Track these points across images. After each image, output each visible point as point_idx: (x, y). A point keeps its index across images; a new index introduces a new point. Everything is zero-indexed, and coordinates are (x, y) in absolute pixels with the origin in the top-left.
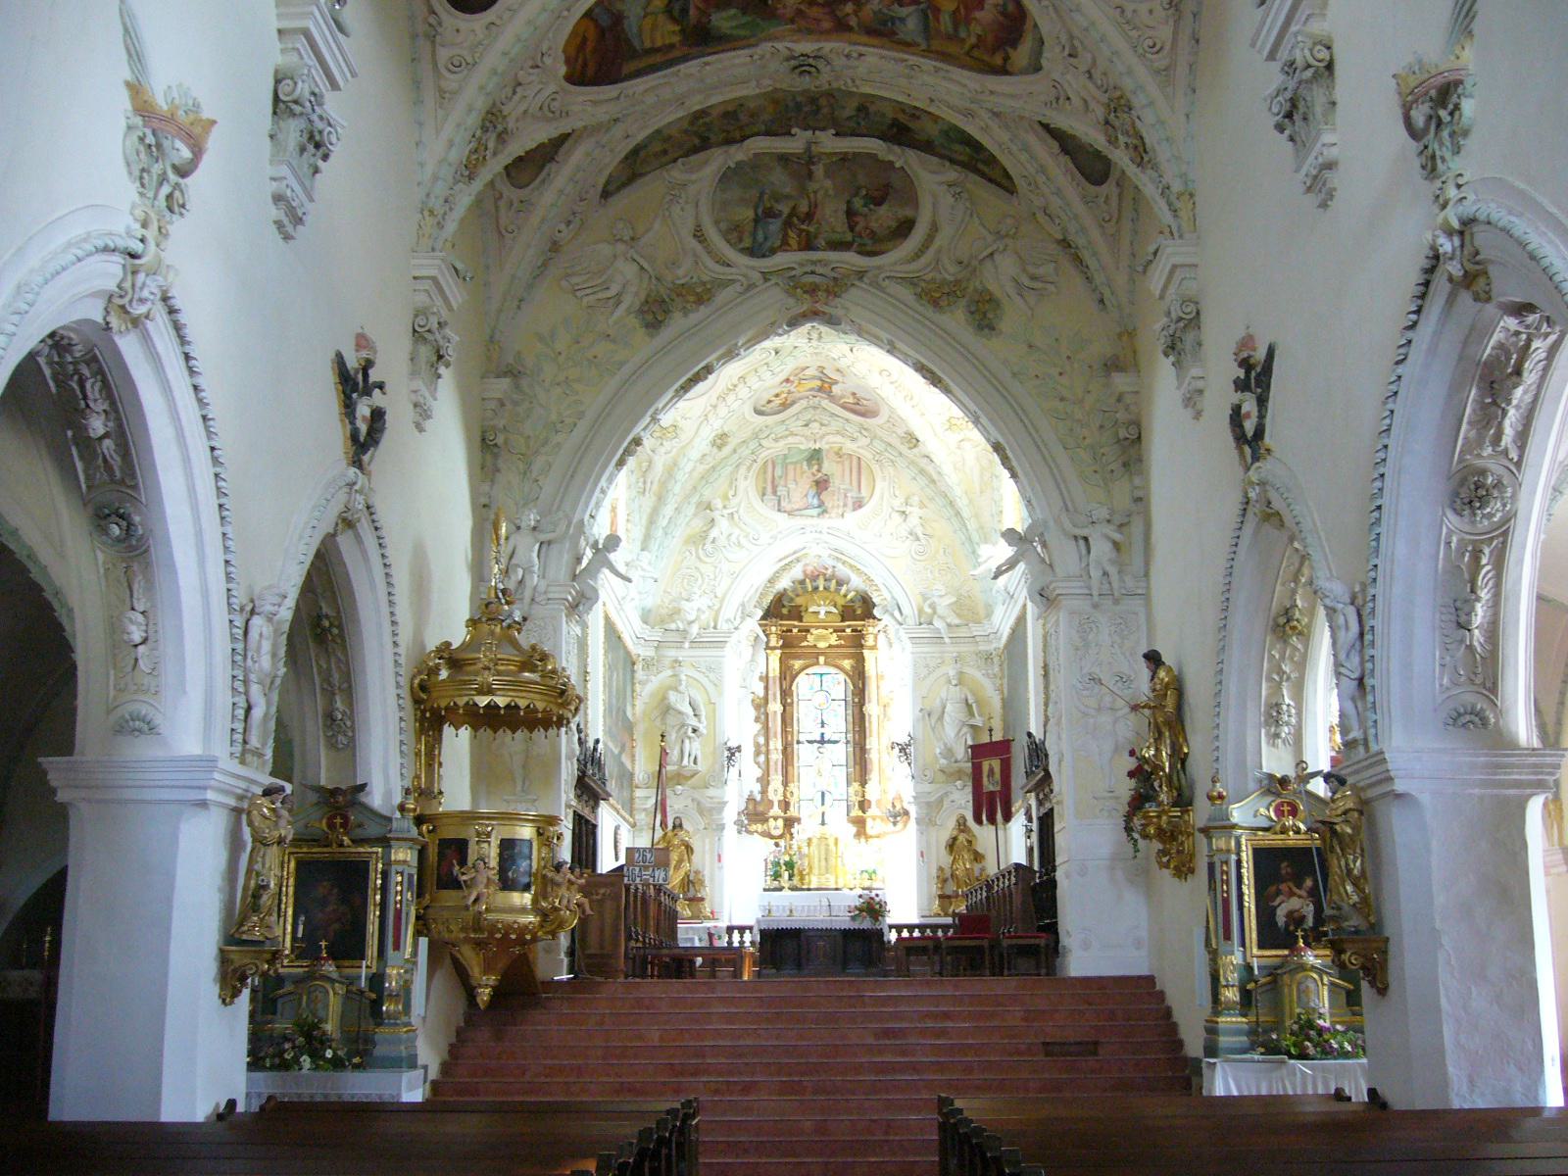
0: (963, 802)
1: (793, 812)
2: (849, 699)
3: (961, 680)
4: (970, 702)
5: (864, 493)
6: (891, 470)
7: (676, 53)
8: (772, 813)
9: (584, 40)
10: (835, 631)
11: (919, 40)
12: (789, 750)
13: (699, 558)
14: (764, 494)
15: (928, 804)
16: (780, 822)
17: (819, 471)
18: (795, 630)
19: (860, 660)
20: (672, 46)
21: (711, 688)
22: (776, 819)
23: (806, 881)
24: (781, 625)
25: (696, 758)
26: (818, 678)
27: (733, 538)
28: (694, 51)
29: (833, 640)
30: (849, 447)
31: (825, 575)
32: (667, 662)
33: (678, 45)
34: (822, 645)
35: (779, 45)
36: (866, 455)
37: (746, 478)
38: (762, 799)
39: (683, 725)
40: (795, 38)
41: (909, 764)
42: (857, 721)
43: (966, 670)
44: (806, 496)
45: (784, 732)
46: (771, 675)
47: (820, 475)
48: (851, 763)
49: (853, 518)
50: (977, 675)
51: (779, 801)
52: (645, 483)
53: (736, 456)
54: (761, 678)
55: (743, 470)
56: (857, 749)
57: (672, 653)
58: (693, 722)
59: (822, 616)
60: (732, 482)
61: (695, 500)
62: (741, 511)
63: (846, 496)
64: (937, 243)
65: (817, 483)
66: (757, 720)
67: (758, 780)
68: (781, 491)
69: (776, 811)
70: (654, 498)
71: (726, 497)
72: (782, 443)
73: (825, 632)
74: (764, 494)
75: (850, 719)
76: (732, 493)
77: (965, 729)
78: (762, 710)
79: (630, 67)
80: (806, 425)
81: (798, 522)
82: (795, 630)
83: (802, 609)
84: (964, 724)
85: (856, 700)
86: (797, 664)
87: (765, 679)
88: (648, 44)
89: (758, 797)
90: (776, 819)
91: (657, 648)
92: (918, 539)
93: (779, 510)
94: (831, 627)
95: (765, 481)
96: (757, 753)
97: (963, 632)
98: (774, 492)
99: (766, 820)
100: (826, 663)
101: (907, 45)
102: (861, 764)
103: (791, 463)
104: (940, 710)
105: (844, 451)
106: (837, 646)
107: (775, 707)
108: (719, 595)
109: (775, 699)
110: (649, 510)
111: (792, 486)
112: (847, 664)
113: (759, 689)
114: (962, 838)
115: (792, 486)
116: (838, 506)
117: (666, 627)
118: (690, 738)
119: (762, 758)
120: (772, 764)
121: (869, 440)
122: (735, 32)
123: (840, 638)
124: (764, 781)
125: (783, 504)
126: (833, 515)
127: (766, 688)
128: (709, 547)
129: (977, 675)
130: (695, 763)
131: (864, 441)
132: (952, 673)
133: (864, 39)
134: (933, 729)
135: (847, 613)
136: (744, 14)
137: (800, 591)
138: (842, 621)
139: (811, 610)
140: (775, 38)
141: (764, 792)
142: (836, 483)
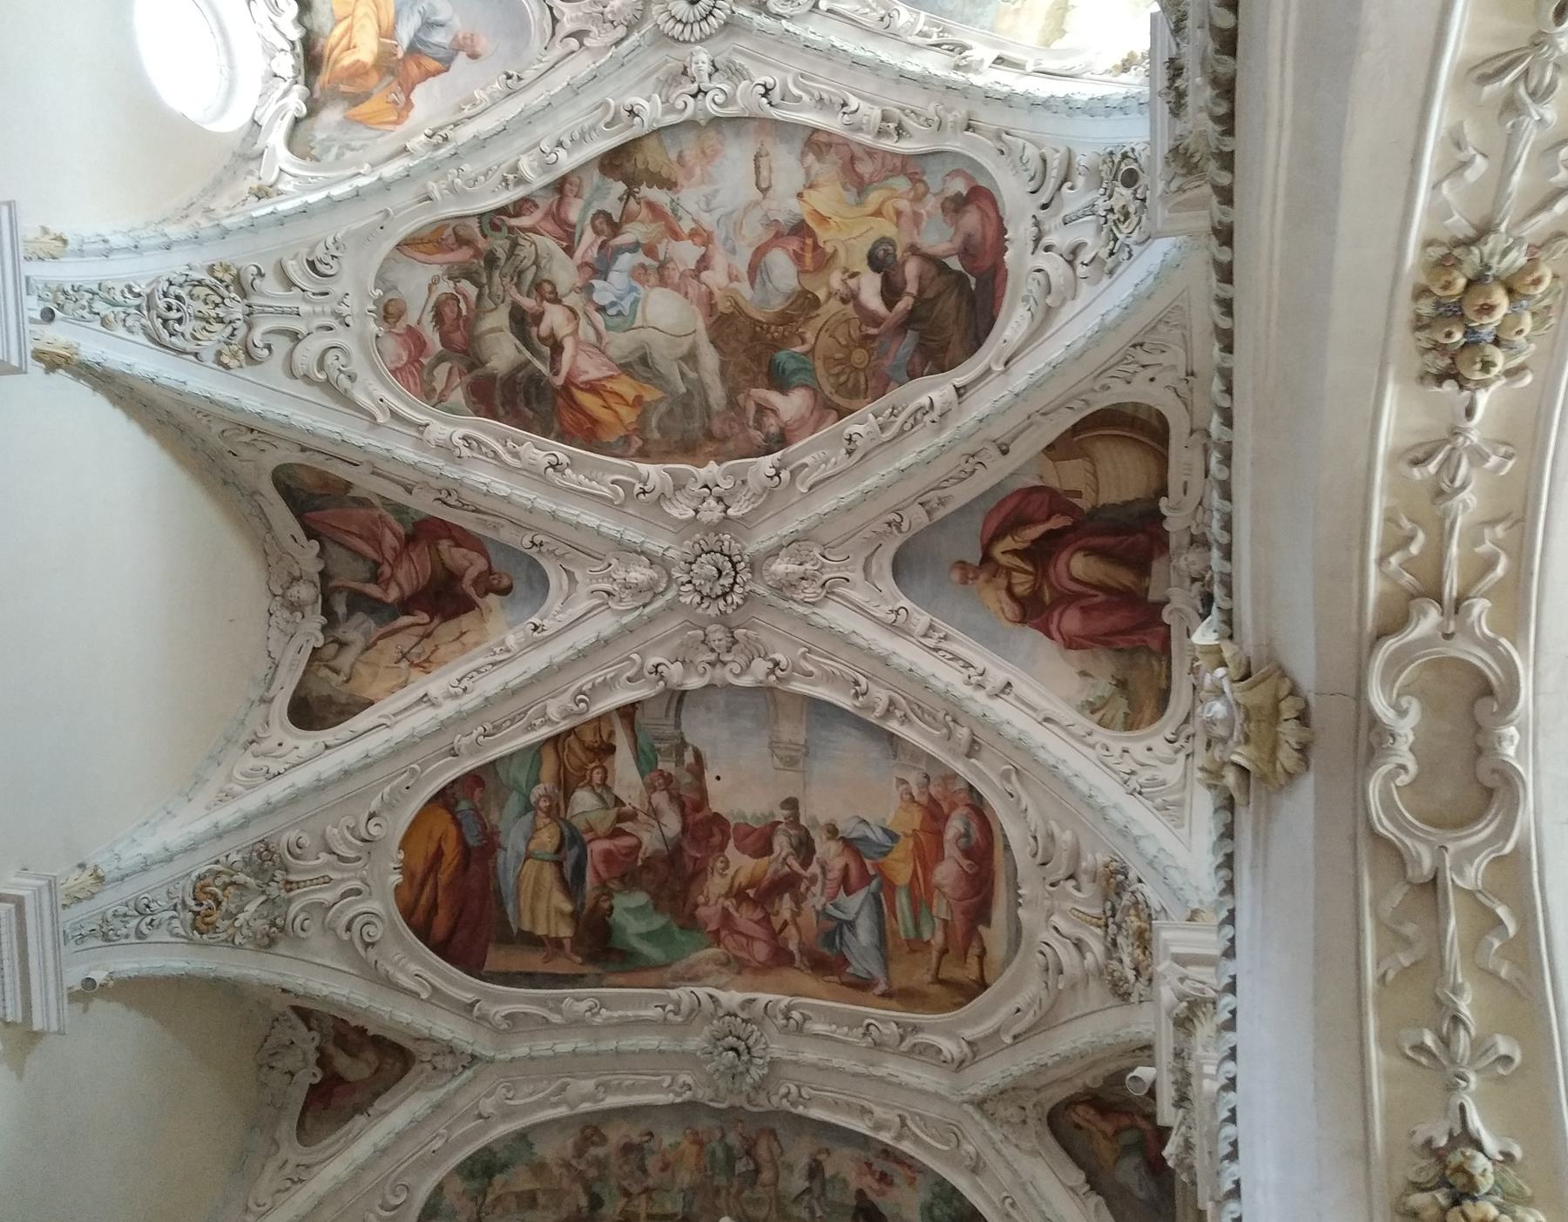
7: (561, 966)
9: (439, 854)
11: (875, 969)
20: (558, 943)
28: (588, 969)
33: (567, 943)
35: (701, 992)
40: (724, 979)
79: (497, 959)
88: (526, 927)
101: (862, 985)
122: (645, 948)
133: (808, 981)
136: (657, 907)
140: (695, 979)
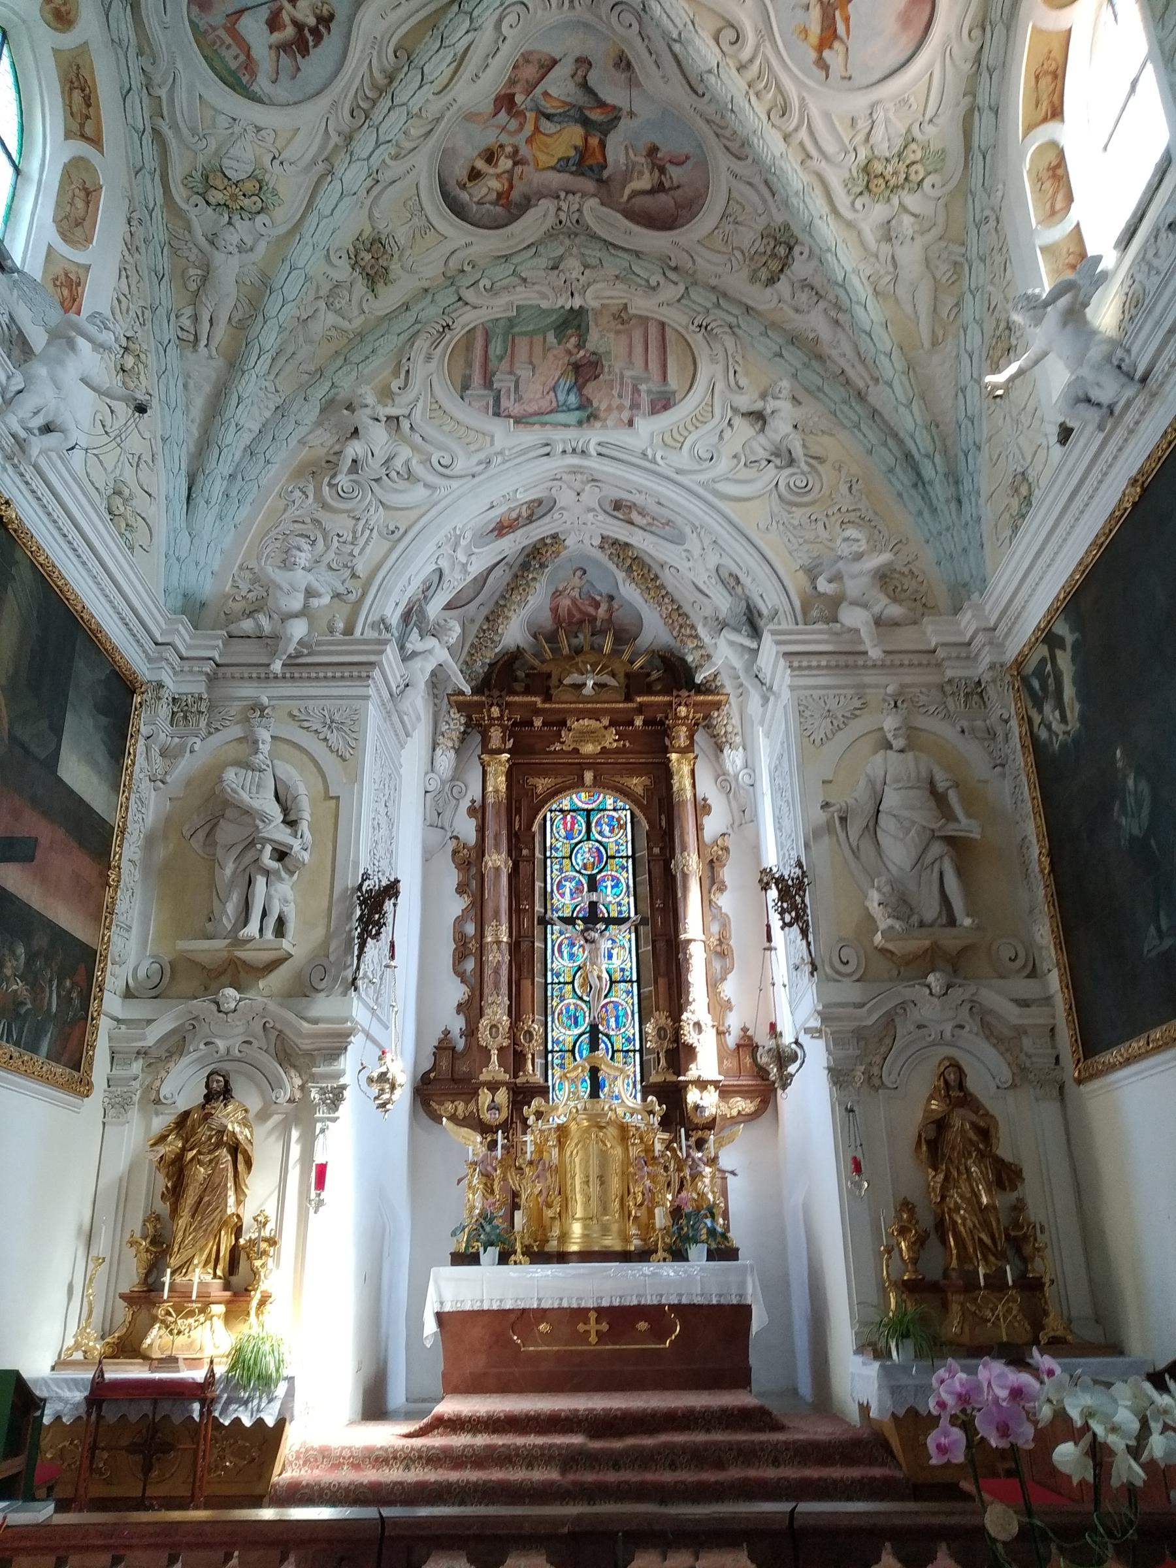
0: (948, 1028)
1: (532, 1073)
2: (643, 853)
3: (913, 739)
4: (941, 786)
5: (673, 383)
6: (729, 342)
8: (484, 1077)
10: (612, 724)
12: (524, 946)
13: (325, 506)
14: (465, 387)
15: (859, 1035)
16: (502, 1096)
17: (580, 346)
18: (538, 722)
19: (664, 775)
21: (328, 761)
22: (493, 1087)
23: (556, 1232)
24: (508, 704)
25: (281, 922)
26: (581, 820)
27: (398, 464)
29: (611, 739)
30: (641, 304)
31: (593, 620)
32: (234, 709)
34: (589, 748)
36: (676, 318)
37: (429, 358)
38: (468, 1047)
39: (252, 844)
41: (804, 933)
42: (658, 889)
43: (921, 722)
44: (554, 389)
45: (516, 912)
46: (490, 800)
47: (582, 353)
48: (649, 974)
49: (648, 427)
50: (946, 731)
51: (501, 1049)
52: (195, 318)
53: (410, 317)
54: (472, 811)
55: (422, 344)
56: (661, 945)
57: (248, 691)
58: (282, 834)
59: (588, 690)
60: (401, 367)
61: (320, 392)
62: (417, 415)
63: (636, 390)
64: (729, 353)
65: (577, 368)
66: (461, 889)
67: (460, 1008)
68: (502, 381)
69: (494, 1070)
70: (219, 362)
71: (386, 394)
72: (503, 300)
73: (594, 724)
74: (465, 387)
75: (645, 889)
76: (400, 382)
77: (937, 848)
78: (473, 871)
80: (554, 268)
81: (530, 437)
82: (538, 722)
83: (554, 681)
84: (933, 837)
85: (656, 850)
86: (542, 784)
87: (478, 811)
89: (461, 1044)
90: (493, 1087)
91: (212, 679)
92: (792, 462)
93: (497, 414)
94: (606, 712)
95: (469, 364)
96: (460, 955)
97: (906, 639)
98: (488, 383)
99: (474, 1094)
100: (600, 784)
102: (668, 974)
103: (524, 334)
104: (870, 808)
105: (632, 311)
106: (617, 751)
107: (497, 860)
108: (361, 569)
109: (497, 846)
110: (207, 388)
111: (524, 373)
112: (637, 783)
113: (467, 829)
114: (959, 1121)
115: (524, 373)
116: (620, 408)
117: (233, 628)
118: (267, 873)
119: (470, 965)
120: (488, 971)
121: (681, 288)
123: (622, 736)
124: (472, 1009)
125: (504, 403)
126: (609, 423)
127: (481, 830)
128: (343, 480)
129: (946, 731)
130: (280, 928)
131: (670, 292)
132: (890, 723)
134: (856, 853)
135: (635, 684)
137: (549, 655)
138: (628, 698)
139: (567, 681)
141: (471, 1032)
142: (616, 365)
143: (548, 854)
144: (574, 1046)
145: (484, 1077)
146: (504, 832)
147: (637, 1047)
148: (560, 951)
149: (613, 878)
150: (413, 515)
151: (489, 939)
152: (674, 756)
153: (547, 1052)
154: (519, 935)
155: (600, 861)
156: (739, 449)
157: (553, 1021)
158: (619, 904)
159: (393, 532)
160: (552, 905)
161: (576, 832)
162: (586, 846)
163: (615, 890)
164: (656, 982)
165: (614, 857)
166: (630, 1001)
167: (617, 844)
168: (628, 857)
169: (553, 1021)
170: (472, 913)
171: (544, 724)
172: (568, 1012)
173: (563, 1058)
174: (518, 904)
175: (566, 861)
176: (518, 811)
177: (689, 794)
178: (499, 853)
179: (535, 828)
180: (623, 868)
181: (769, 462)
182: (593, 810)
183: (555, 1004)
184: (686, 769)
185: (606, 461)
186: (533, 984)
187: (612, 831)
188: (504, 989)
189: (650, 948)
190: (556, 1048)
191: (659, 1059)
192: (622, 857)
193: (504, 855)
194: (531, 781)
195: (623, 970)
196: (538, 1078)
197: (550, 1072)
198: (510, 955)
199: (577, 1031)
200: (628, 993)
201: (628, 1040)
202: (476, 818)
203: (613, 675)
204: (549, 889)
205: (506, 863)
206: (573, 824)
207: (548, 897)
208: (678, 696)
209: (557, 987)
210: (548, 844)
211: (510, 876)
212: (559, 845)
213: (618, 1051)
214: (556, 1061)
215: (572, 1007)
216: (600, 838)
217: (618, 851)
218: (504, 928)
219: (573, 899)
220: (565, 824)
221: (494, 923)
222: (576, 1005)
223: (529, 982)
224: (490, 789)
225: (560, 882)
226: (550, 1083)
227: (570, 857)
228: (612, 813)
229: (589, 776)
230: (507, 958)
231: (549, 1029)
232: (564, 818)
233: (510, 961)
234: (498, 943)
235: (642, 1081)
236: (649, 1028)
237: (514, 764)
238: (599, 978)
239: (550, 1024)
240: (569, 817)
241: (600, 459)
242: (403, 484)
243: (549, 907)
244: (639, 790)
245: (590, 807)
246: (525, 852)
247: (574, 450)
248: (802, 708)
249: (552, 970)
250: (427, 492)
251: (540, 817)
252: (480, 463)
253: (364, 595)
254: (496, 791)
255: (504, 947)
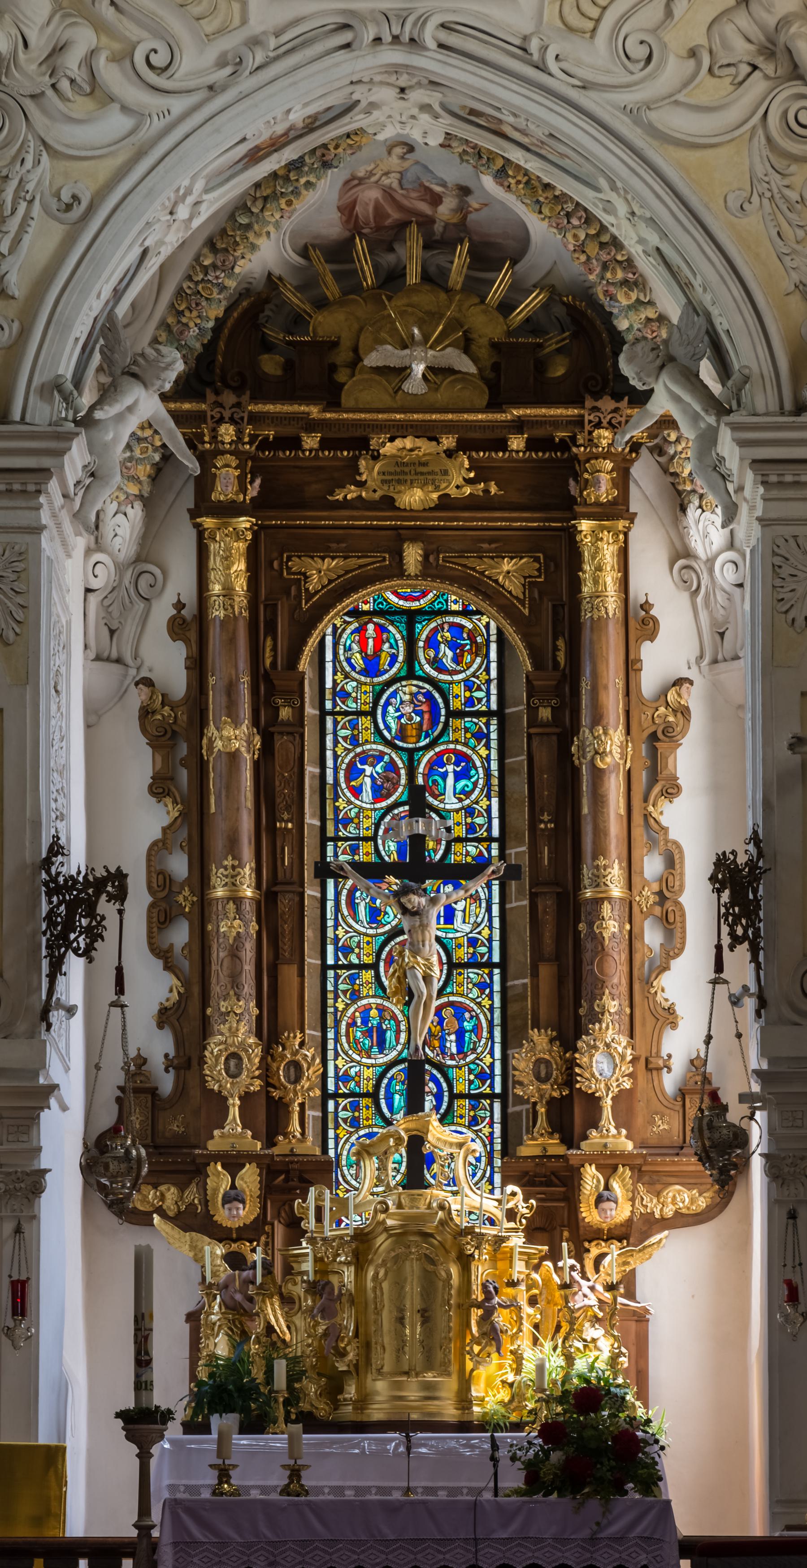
2: (517, 709)
8: (216, 1144)
10: (464, 445)
12: (285, 903)
18: (311, 442)
24: (254, 418)
27: (72, 62)
31: (426, 223)
38: (181, 1088)
42: (546, 793)
46: (217, 613)
48: (522, 954)
51: (246, 1098)
56: (547, 904)
73: (426, 447)
75: (519, 786)
78: (183, 750)
83: (343, 355)
85: (545, 713)
89: (166, 1083)
94: (448, 428)
102: (558, 957)
106: (471, 504)
120: (219, 954)
123: (482, 473)
137: (332, 289)
138: (494, 405)
139: (372, 359)
143: (329, 705)
144: (377, 1086)
145: (216, 1144)
146: (245, 680)
147: (498, 1089)
148: (352, 904)
149: (461, 757)
150: (105, 169)
151: (220, 892)
152: (585, 525)
153: (326, 1096)
154: (274, 880)
155: (434, 721)
156: (701, 39)
157: (337, 1040)
158: (470, 811)
159: (69, 207)
160: (337, 810)
161: (385, 660)
162: (407, 689)
163: (462, 783)
164: (535, 974)
165: (460, 714)
166: (486, 1003)
167: (469, 686)
168: (489, 714)
169: (337, 1040)
170: (183, 834)
171: (324, 444)
172: (365, 1021)
173: (355, 1107)
174: (273, 818)
175: (365, 722)
176: (271, 629)
177: (612, 604)
178: (236, 724)
179: (305, 664)
180: (480, 736)
181: (755, 68)
182: (420, 612)
183: (340, 1006)
184: (609, 552)
185: (454, 60)
186: (301, 974)
187: (457, 660)
188: (248, 987)
189: (526, 903)
190: (343, 1090)
191: (535, 1114)
192: (478, 714)
193: (245, 727)
194: (295, 564)
195: (473, 942)
196: (310, 1146)
197: (331, 1133)
198: (259, 922)
199: (383, 1059)
200: (482, 986)
201: (483, 1077)
202: (187, 642)
203: (467, 346)
204: (330, 779)
205: (249, 742)
206: (379, 643)
207: (329, 795)
208: (595, 409)
209: (344, 973)
210: (329, 684)
211: (256, 765)
212: (350, 686)
213: (461, 1096)
214: (342, 1114)
215: (374, 1013)
216: (434, 673)
217: (470, 701)
218: (247, 871)
219: (377, 798)
220: (363, 643)
221: (228, 862)
222: (381, 1009)
223: (293, 969)
224: (217, 588)
225: (351, 765)
226: (332, 1153)
227: (372, 714)
228: (458, 620)
229: (413, 555)
230: (254, 927)
231: (331, 1055)
232: (361, 630)
233: (259, 933)
234: (237, 901)
235: (504, 1153)
236: (522, 1062)
237: (262, 527)
238: (427, 979)
239: (331, 1045)
240: (371, 627)
241: (442, 56)
242: (81, 105)
243: (330, 815)
244: (514, 586)
245: (415, 605)
246: (285, 713)
247: (396, 39)
248: (778, 561)
249: (336, 939)
250: (124, 123)
251: (312, 642)
252: (221, 63)
253: (24, 334)
254: (228, 592)
255: (248, 908)
